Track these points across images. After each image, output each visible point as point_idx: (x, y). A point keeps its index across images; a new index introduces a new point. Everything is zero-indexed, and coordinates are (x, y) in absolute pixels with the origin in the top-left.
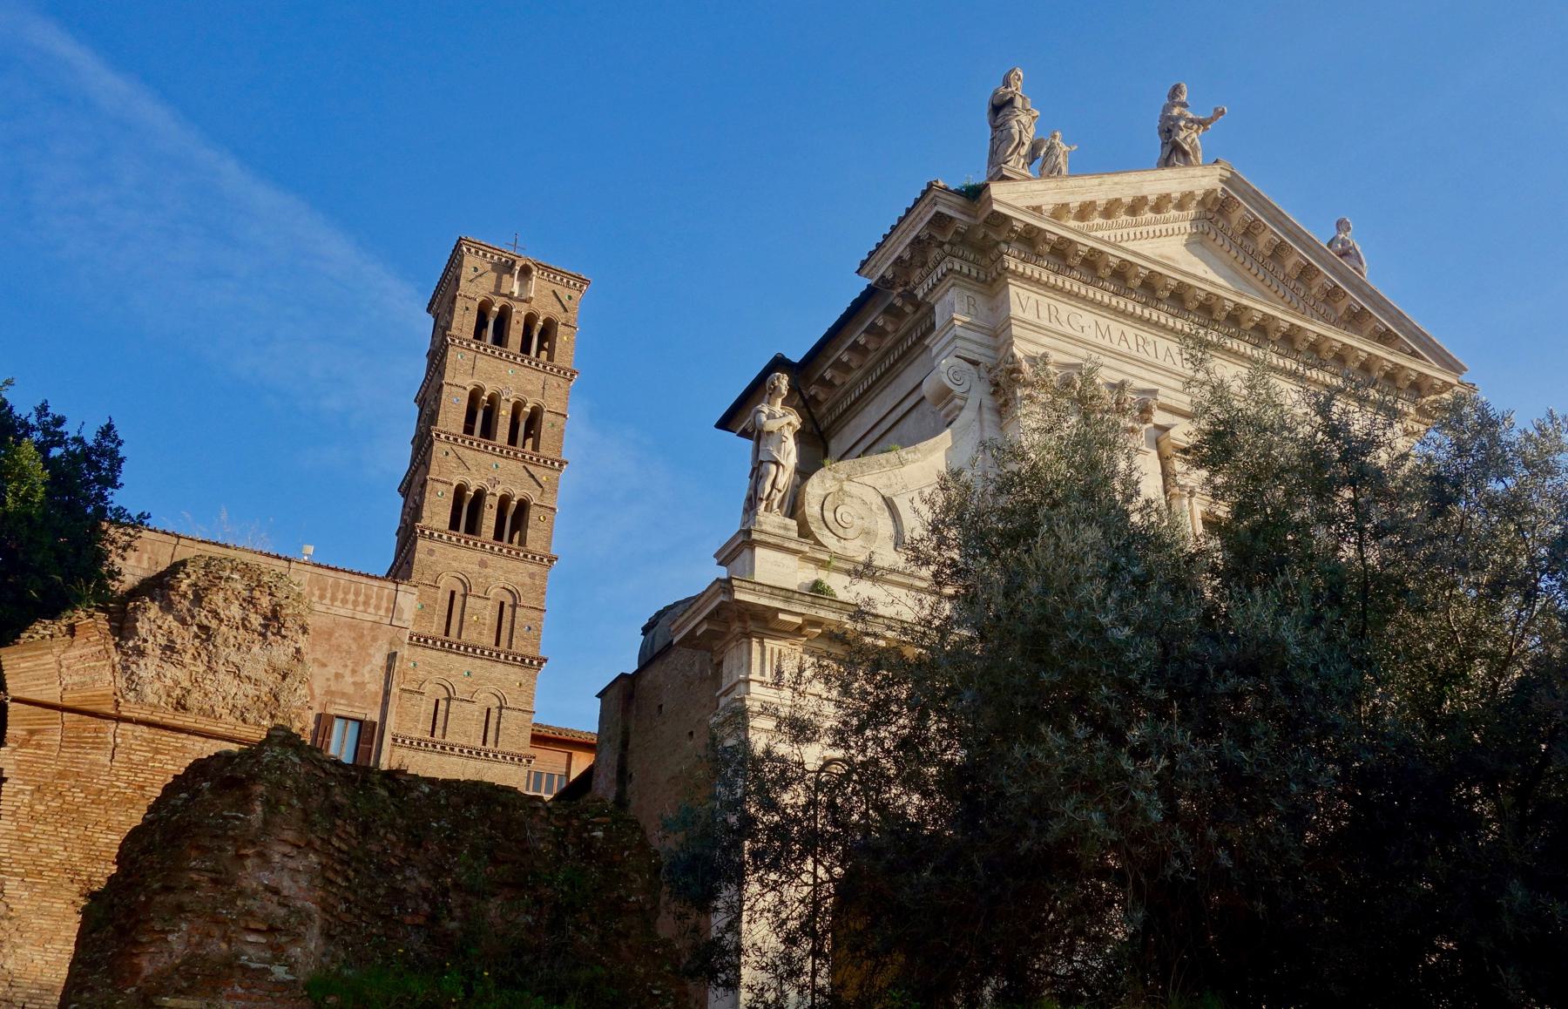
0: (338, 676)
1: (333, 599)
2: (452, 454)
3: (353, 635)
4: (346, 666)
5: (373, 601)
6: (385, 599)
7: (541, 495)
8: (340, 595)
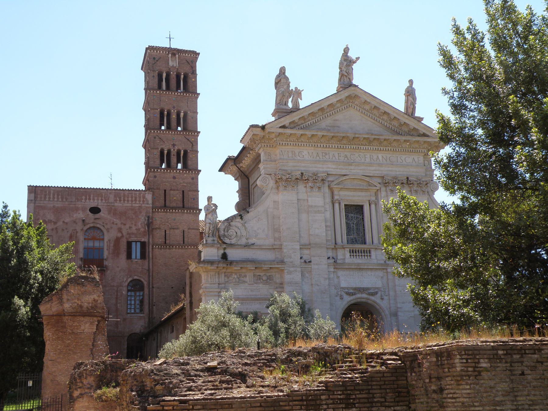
0: (130, 227)
1: (124, 200)
2: (157, 137)
3: (133, 212)
4: (132, 224)
5: (138, 199)
6: (142, 197)
7: (192, 147)
8: (126, 199)
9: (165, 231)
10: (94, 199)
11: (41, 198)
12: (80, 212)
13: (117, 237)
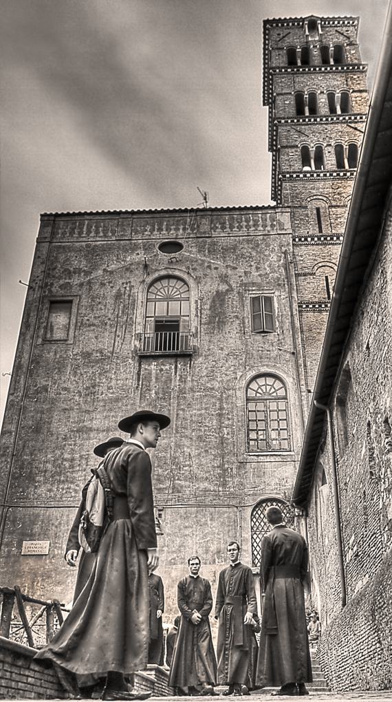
1: (231, 227)
4: (251, 266)
9: (327, 277)
10: (168, 229)
11: (64, 233)
12: (141, 252)
13: (217, 292)
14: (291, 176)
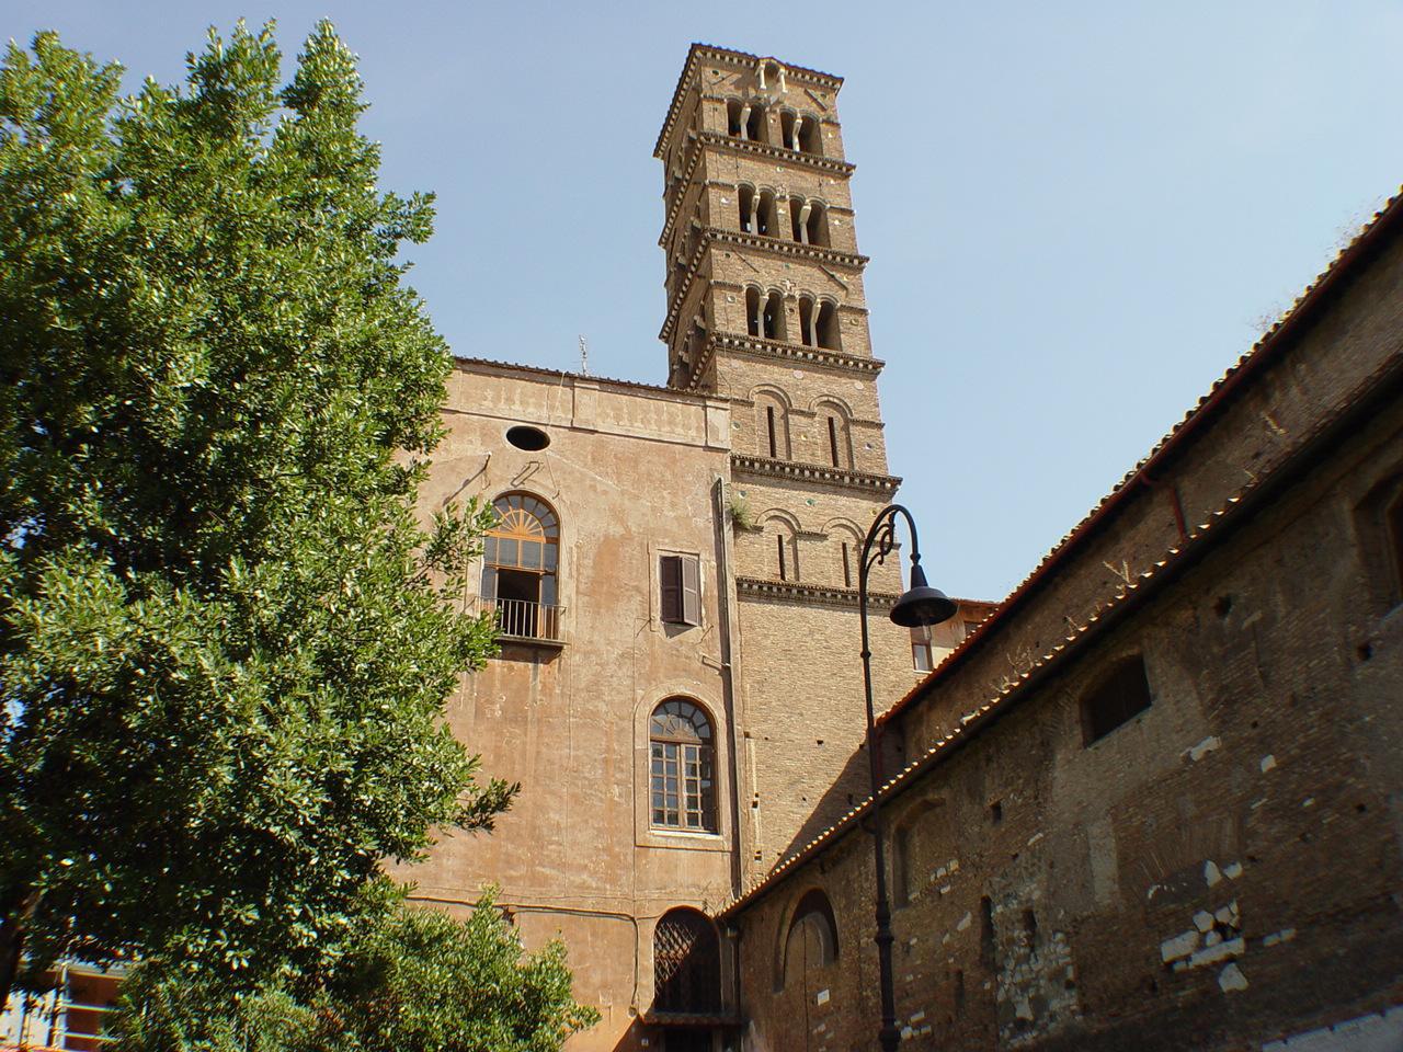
7: (847, 296)
13: (606, 537)
14: (731, 342)
